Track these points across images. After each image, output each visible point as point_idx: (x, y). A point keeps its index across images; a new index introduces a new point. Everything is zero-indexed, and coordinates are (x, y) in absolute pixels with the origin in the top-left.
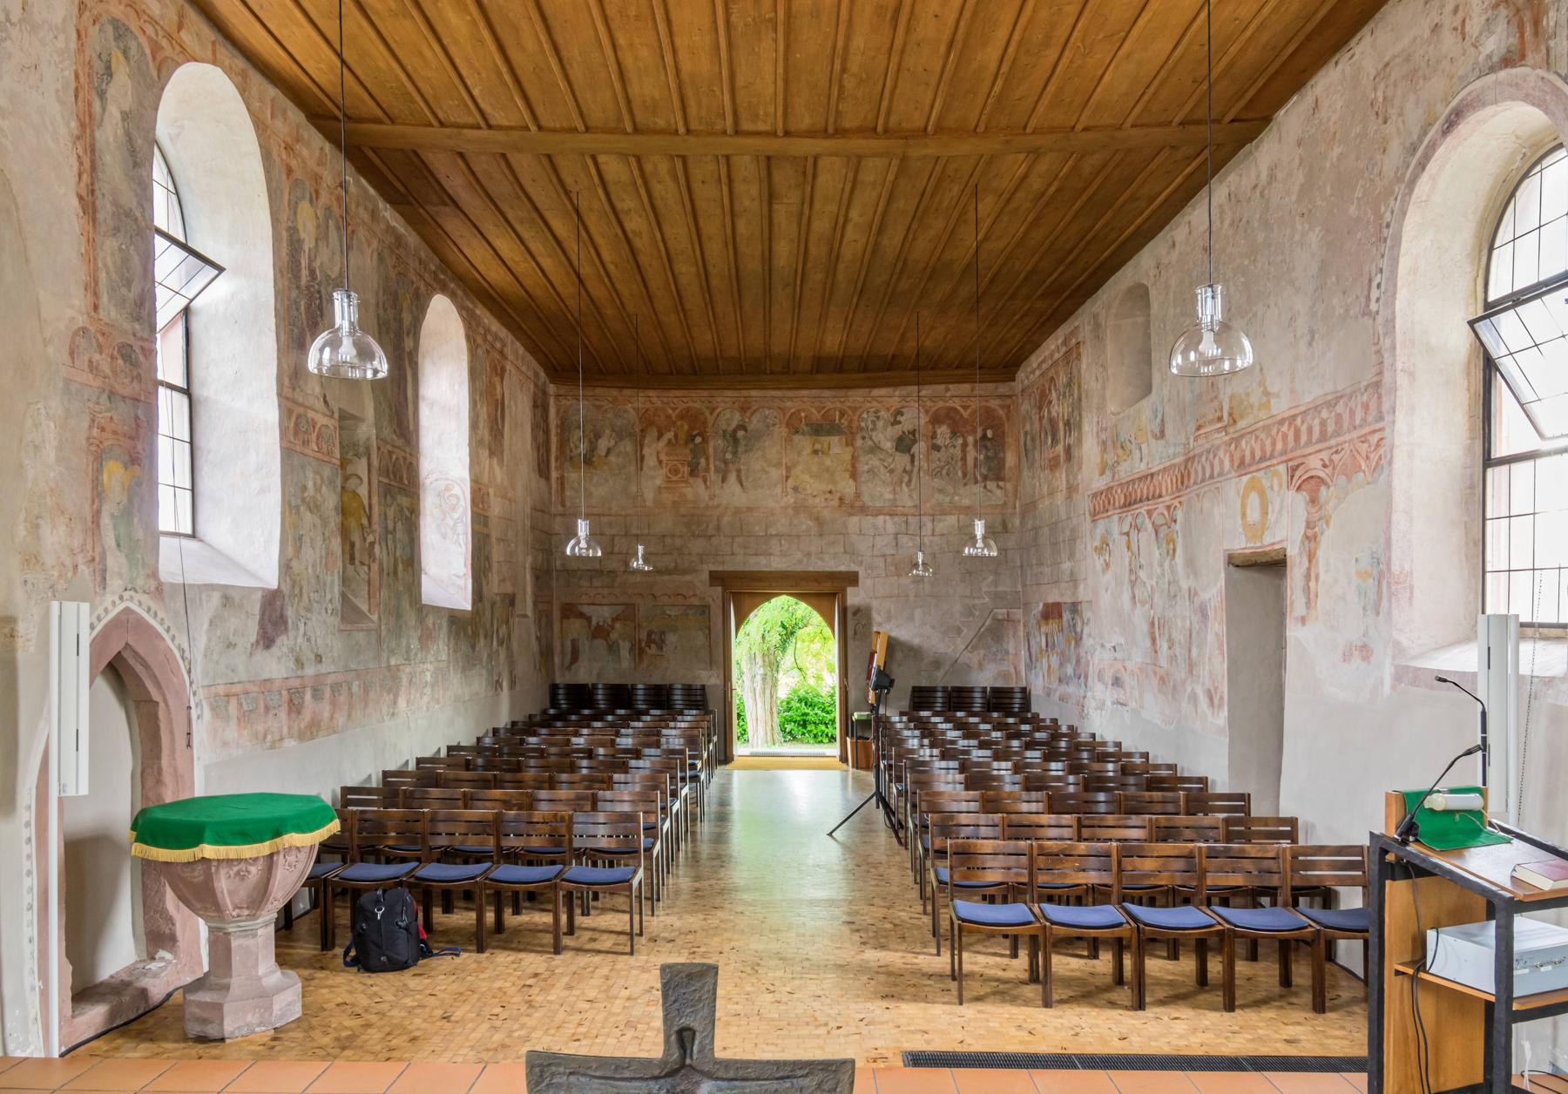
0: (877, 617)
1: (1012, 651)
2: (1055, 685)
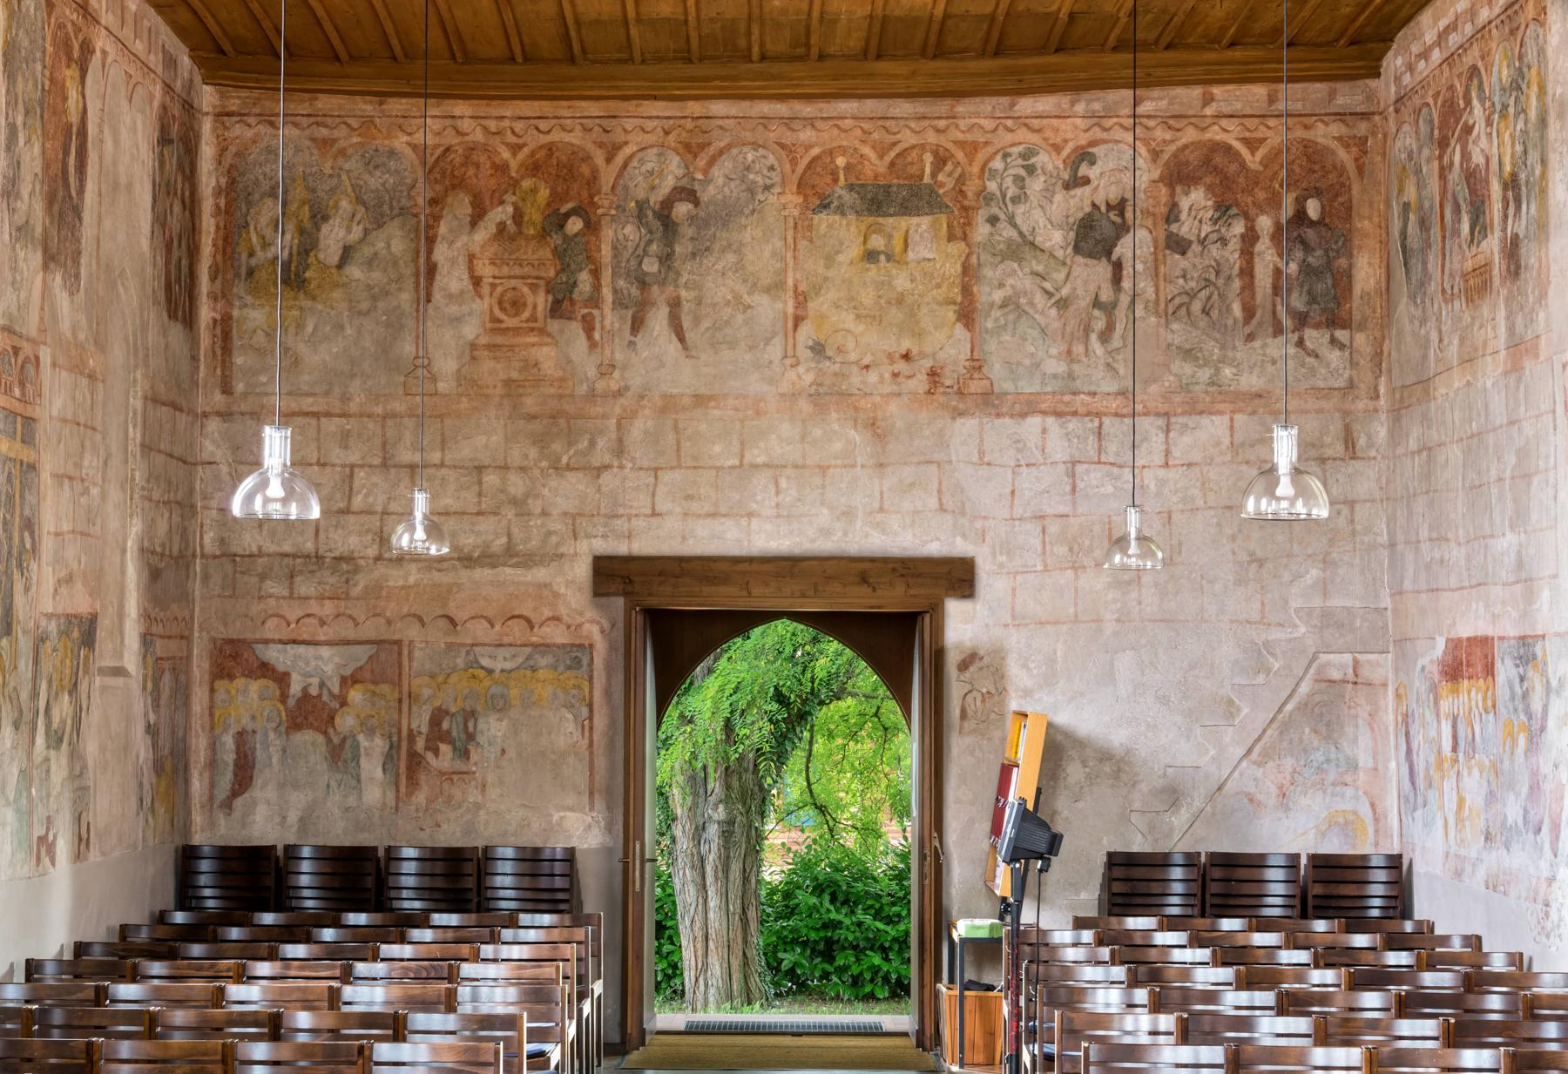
0: (1018, 675)
1: (1365, 760)
2: (1475, 847)
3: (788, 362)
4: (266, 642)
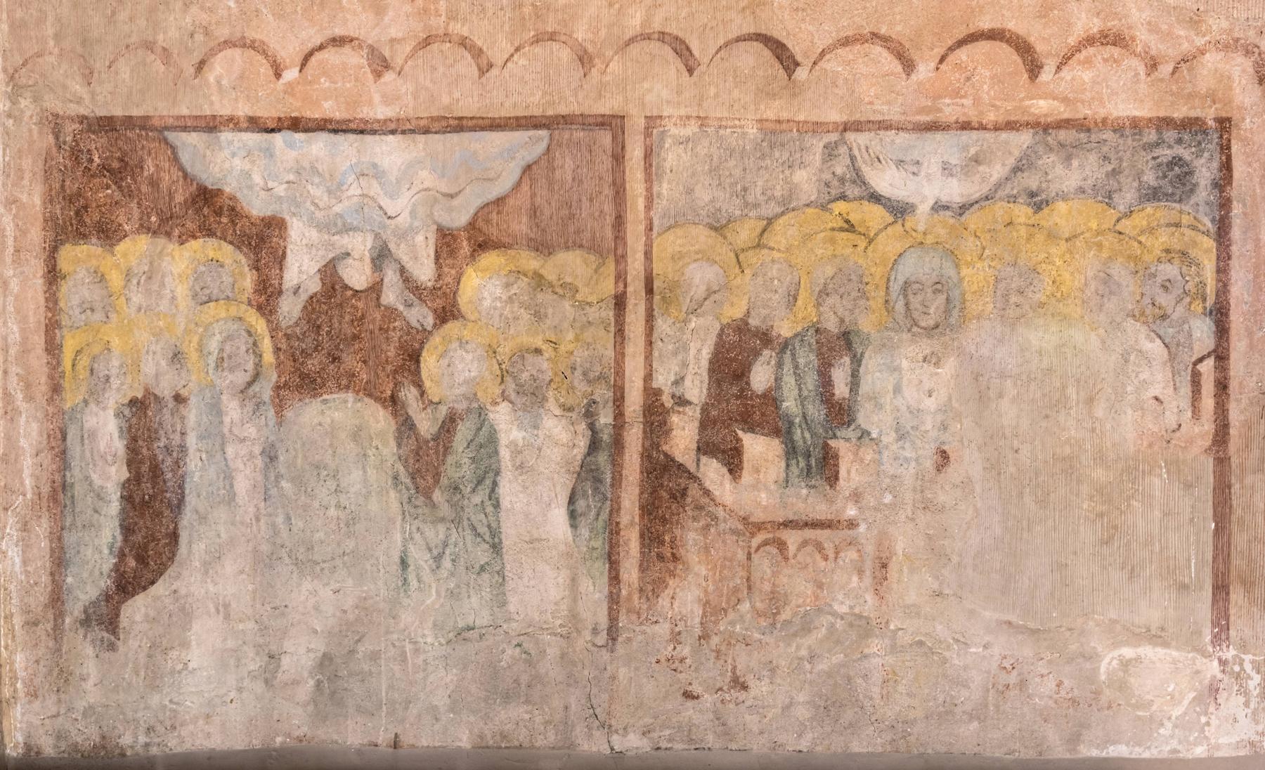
4: (211, 125)
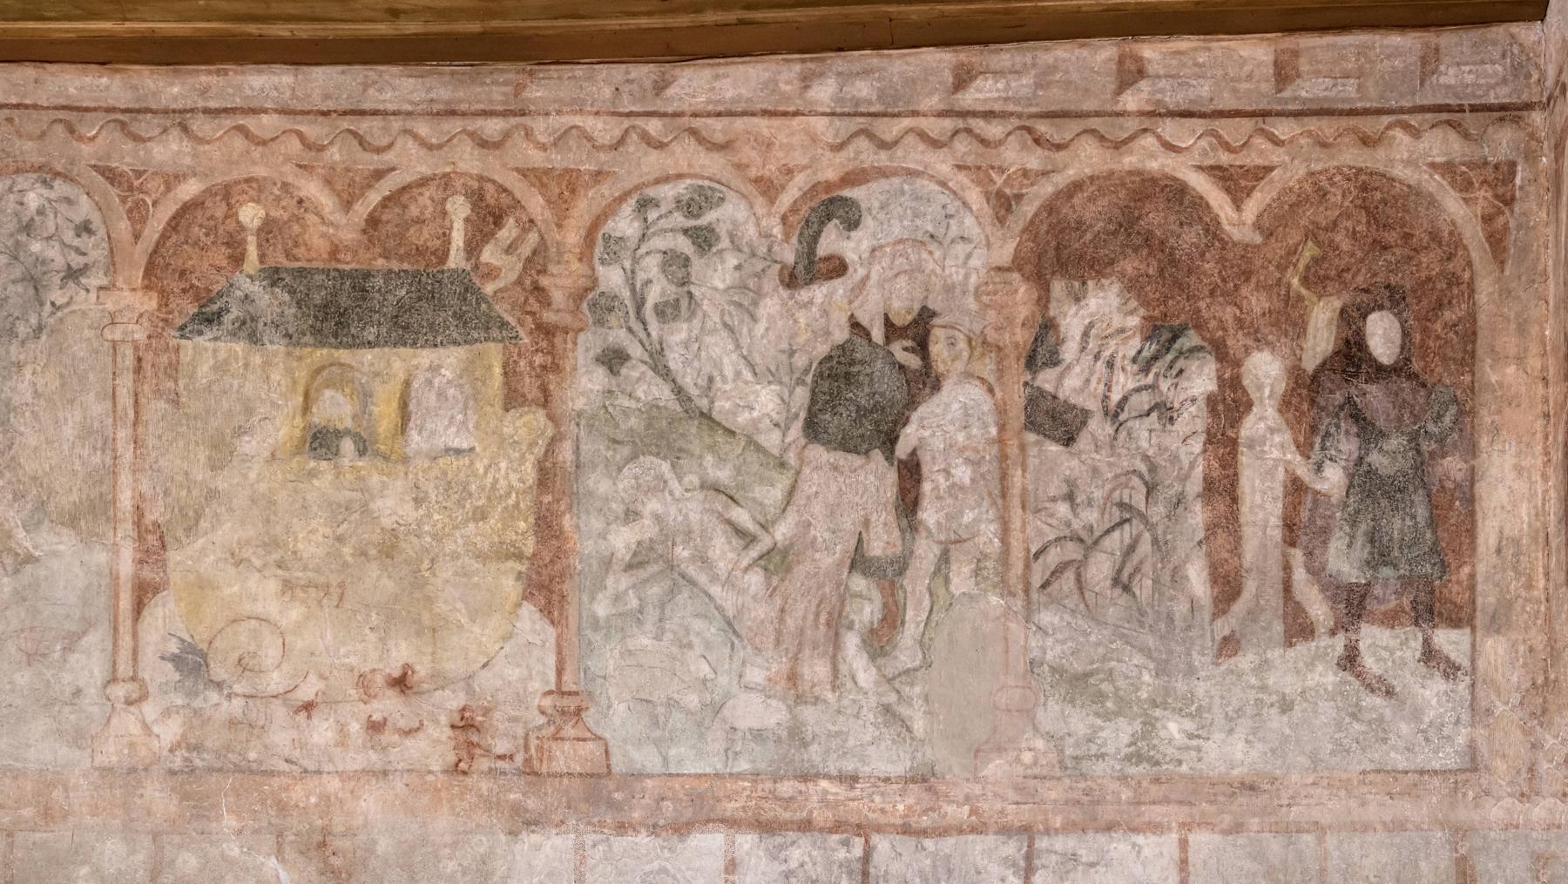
3: (119, 691)
